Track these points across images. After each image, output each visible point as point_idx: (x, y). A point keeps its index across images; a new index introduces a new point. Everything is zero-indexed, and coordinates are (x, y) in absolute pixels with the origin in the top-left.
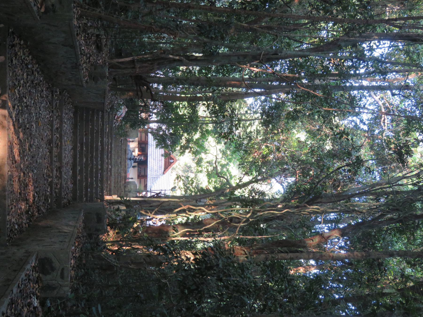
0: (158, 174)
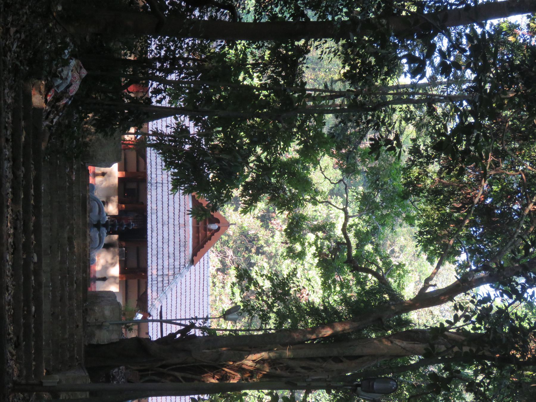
0: (177, 263)
